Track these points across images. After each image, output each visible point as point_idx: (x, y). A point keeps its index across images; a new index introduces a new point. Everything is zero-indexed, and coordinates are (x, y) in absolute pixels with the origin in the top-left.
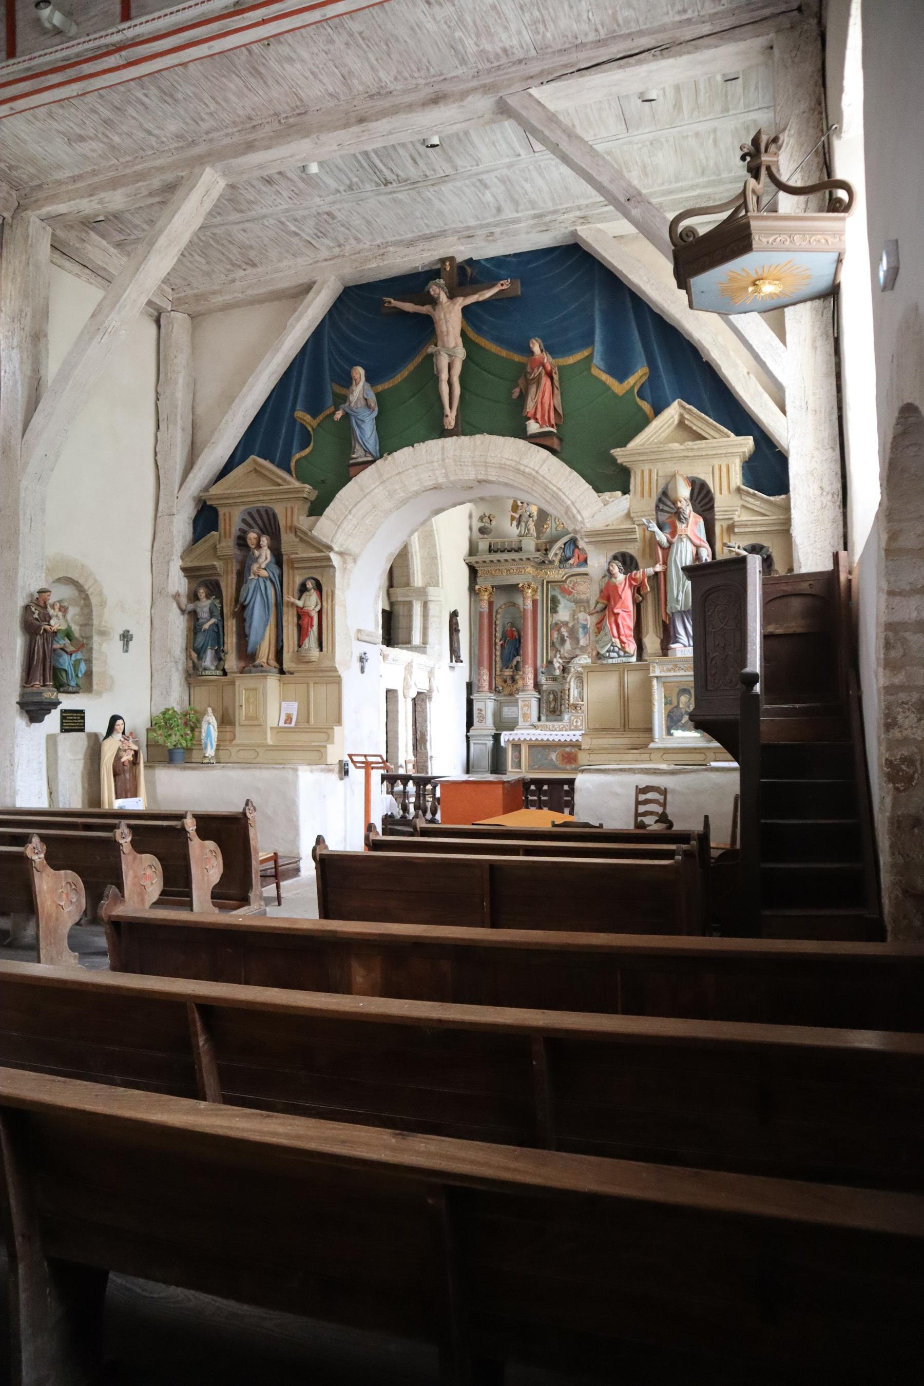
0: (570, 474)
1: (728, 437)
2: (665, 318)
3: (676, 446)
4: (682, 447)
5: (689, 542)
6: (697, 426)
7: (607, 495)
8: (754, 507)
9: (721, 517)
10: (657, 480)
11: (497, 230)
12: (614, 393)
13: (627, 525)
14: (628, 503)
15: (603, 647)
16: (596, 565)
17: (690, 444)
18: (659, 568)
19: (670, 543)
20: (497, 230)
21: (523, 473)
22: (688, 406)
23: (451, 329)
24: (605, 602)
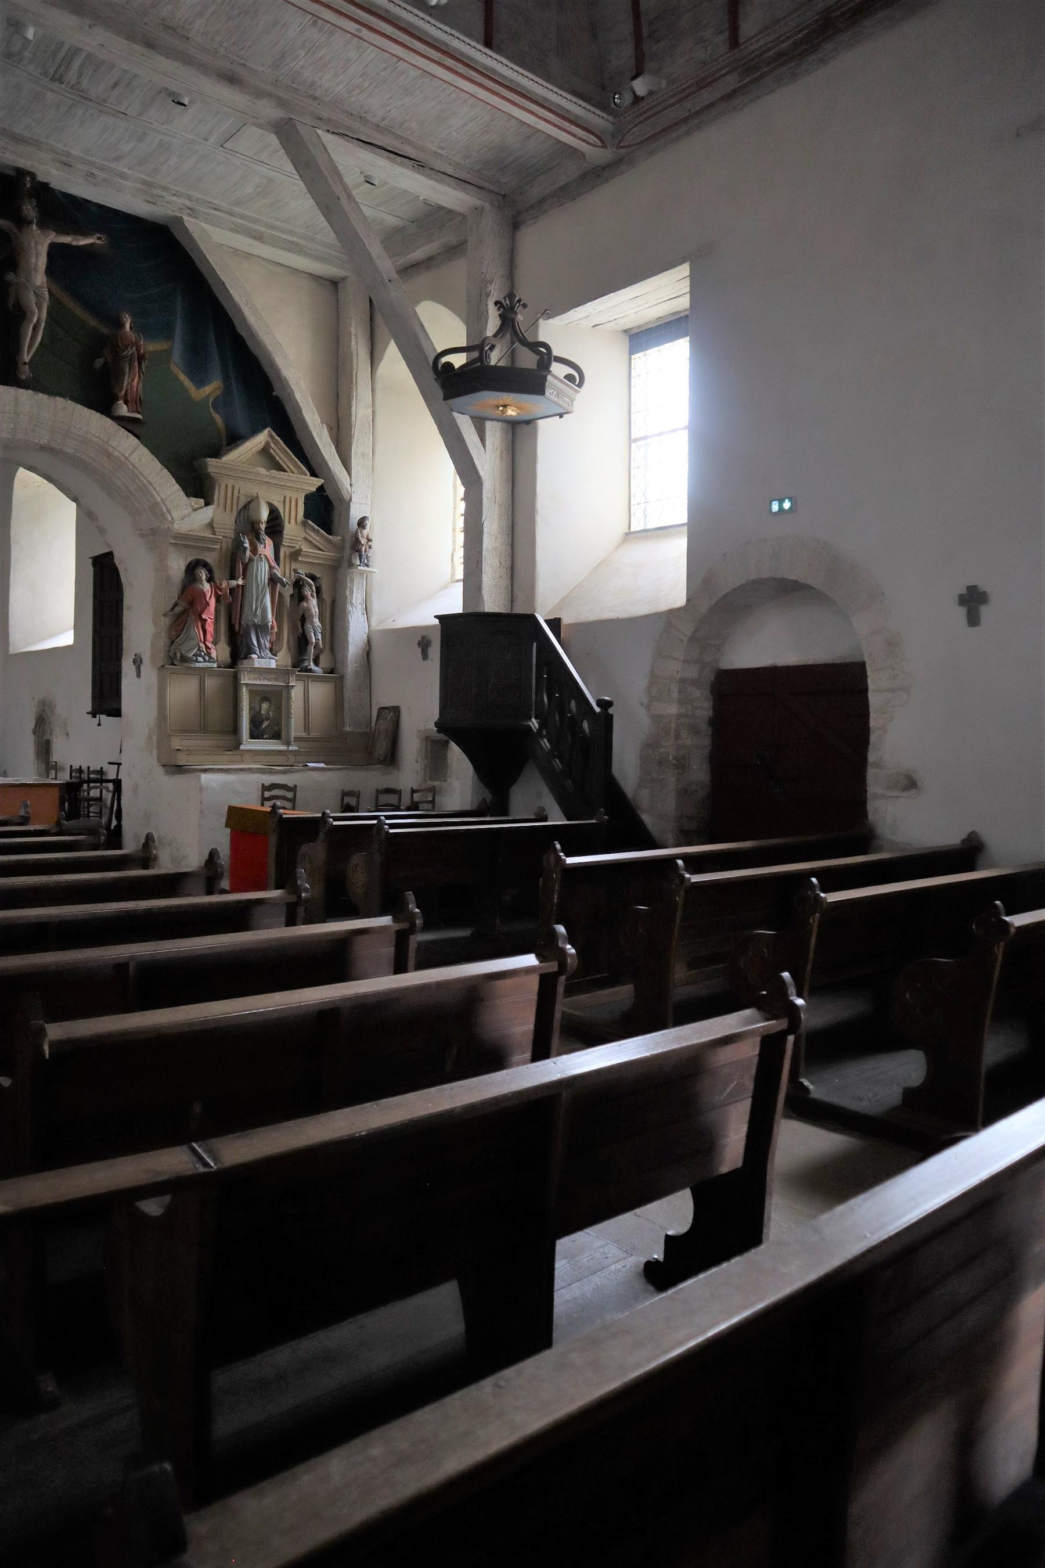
1: (306, 475)
2: (249, 343)
3: (263, 471)
6: (280, 458)
7: (193, 500)
8: (314, 541)
10: (238, 497)
11: (100, 174)
13: (208, 534)
15: (190, 650)
16: (176, 568)
18: (240, 582)
20: (100, 174)
21: (109, 455)
22: (276, 437)
23: (40, 263)
24: (187, 606)
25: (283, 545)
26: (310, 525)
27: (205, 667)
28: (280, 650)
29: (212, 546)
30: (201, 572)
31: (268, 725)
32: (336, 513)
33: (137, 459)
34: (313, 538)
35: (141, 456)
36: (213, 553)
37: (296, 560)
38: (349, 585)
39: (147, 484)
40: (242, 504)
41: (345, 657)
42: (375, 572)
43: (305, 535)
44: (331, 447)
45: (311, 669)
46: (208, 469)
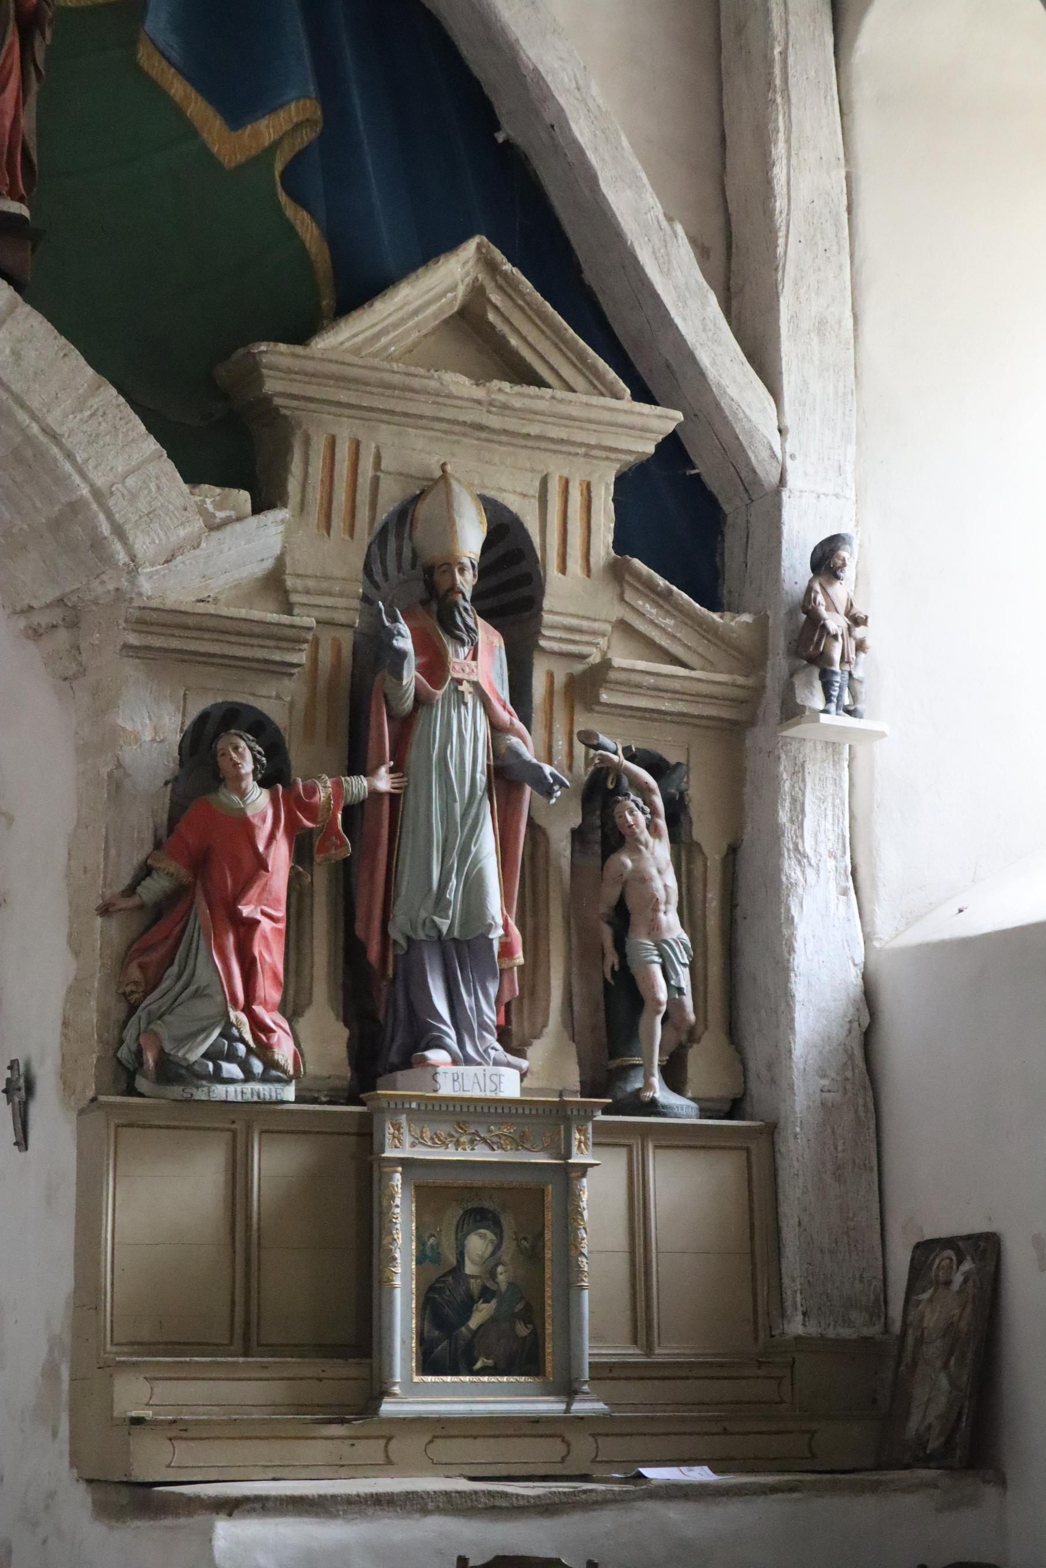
0: (95, 389)
1: (617, 396)
3: (459, 384)
4: (479, 393)
5: (480, 712)
6: (524, 339)
7: (210, 494)
9: (555, 646)
10: (376, 481)
12: (205, 150)
14: (279, 539)
15: (192, 1036)
16: (147, 736)
17: (505, 390)
18: (384, 782)
19: (422, 701)
22: (508, 267)
24: (184, 875)
25: (543, 650)
26: (637, 575)
27: (248, 1097)
28: (537, 1036)
29: (277, 657)
30: (236, 748)
31: (493, 1320)
32: (732, 541)
33: (8, 351)
34: (652, 622)
35: (20, 341)
36: (286, 681)
37: (591, 703)
38: (787, 786)
39: (42, 438)
40: (386, 508)
41: (781, 1053)
42: (882, 735)
43: (618, 612)
44: (704, 305)
45: (653, 1102)
46: (259, 380)
